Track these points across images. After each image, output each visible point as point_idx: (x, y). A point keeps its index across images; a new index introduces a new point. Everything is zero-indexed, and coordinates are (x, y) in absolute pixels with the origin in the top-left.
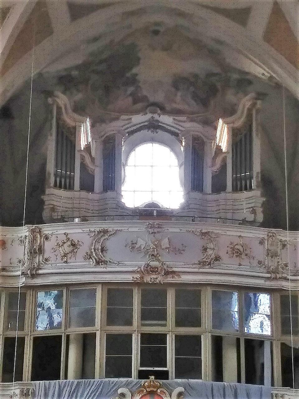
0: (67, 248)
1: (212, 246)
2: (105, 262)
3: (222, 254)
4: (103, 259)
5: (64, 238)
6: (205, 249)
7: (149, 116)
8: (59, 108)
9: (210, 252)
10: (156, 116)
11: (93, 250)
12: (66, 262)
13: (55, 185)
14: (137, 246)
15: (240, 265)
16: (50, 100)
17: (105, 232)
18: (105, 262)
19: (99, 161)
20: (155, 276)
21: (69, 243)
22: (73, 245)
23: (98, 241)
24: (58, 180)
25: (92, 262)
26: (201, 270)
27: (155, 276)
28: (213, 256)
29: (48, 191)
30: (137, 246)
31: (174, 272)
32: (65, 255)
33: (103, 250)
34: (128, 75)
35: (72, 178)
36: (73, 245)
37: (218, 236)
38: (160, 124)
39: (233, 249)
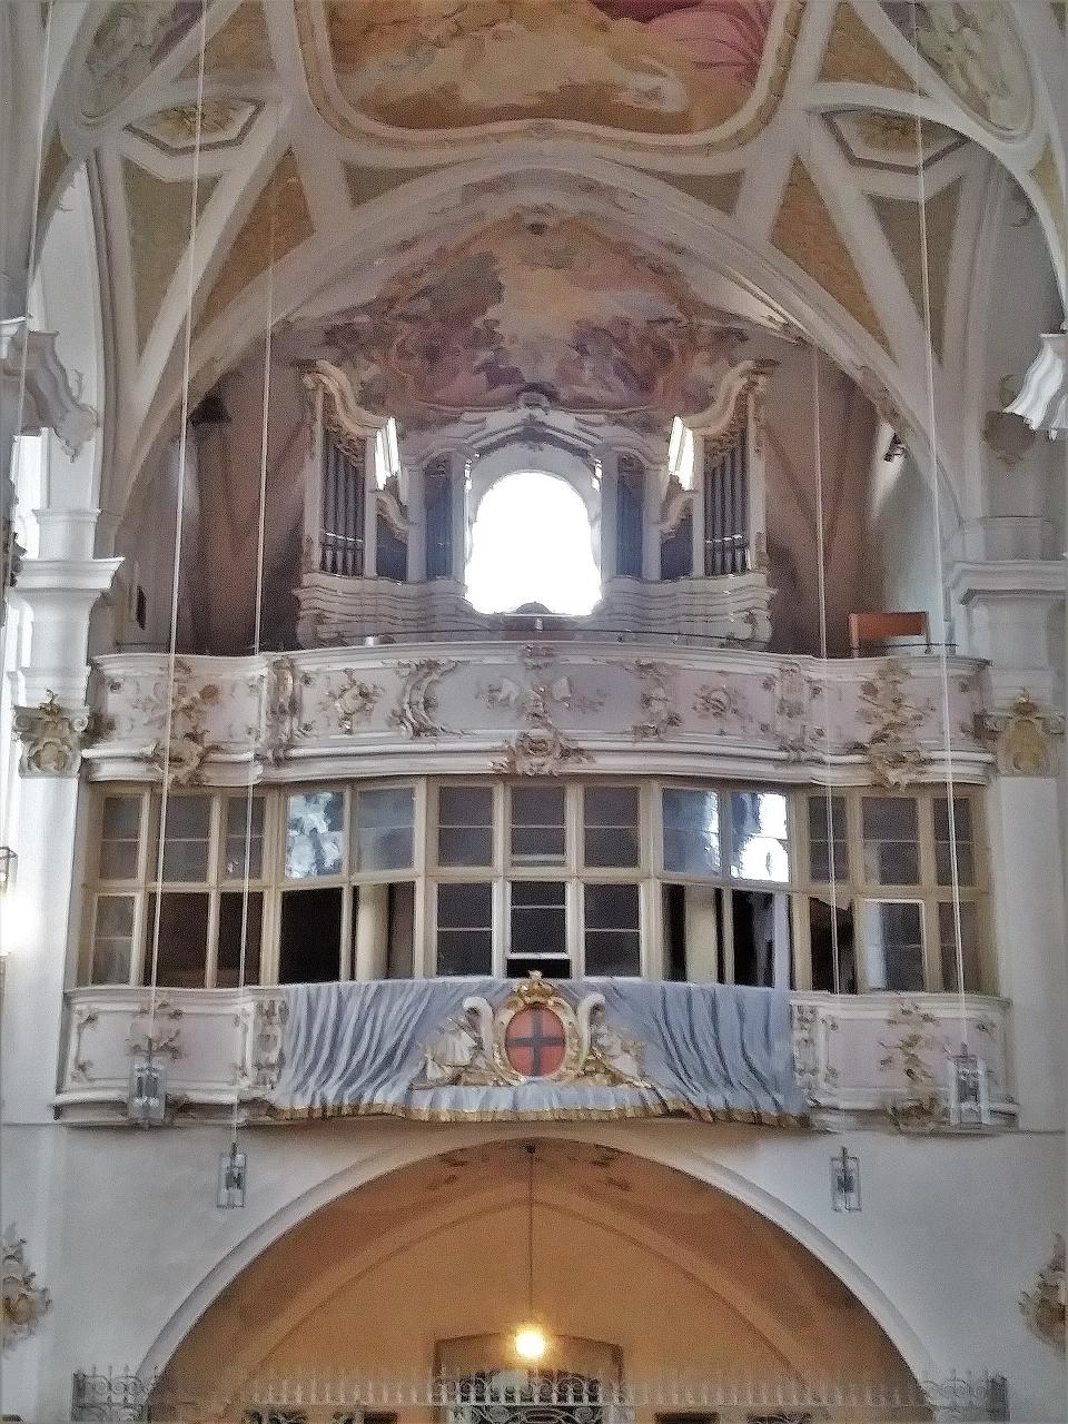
0: (350, 701)
1: (660, 693)
2: (433, 731)
3: (684, 711)
4: (430, 724)
5: (344, 680)
6: (647, 701)
7: (523, 413)
8: (328, 397)
9: (657, 706)
10: (538, 413)
11: (406, 706)
12: (349, 732)
13: (323, 567)
14: (501, 696)
15: (722, 733)
16: (308, 380)
17: (432, 666)
18: (433, 731)
19: (417, 512)
20: (540, 761)
21: (355, 691)
22: (364, 695)
23: (416, 687)
24: (329, 553)
25: (406, 731)
26: (639, 746)
27: (540, 761)
28: (664, 716)
29: (306, 579)
30: (501, 696)
31: (580, 751)
32: (347, 716)
33: (428, 705)
34: (478, 323)
35: (358, 551)
36: (364, 695)
37: (675, 670)
38: (548, 431)
39: (706, 699)
